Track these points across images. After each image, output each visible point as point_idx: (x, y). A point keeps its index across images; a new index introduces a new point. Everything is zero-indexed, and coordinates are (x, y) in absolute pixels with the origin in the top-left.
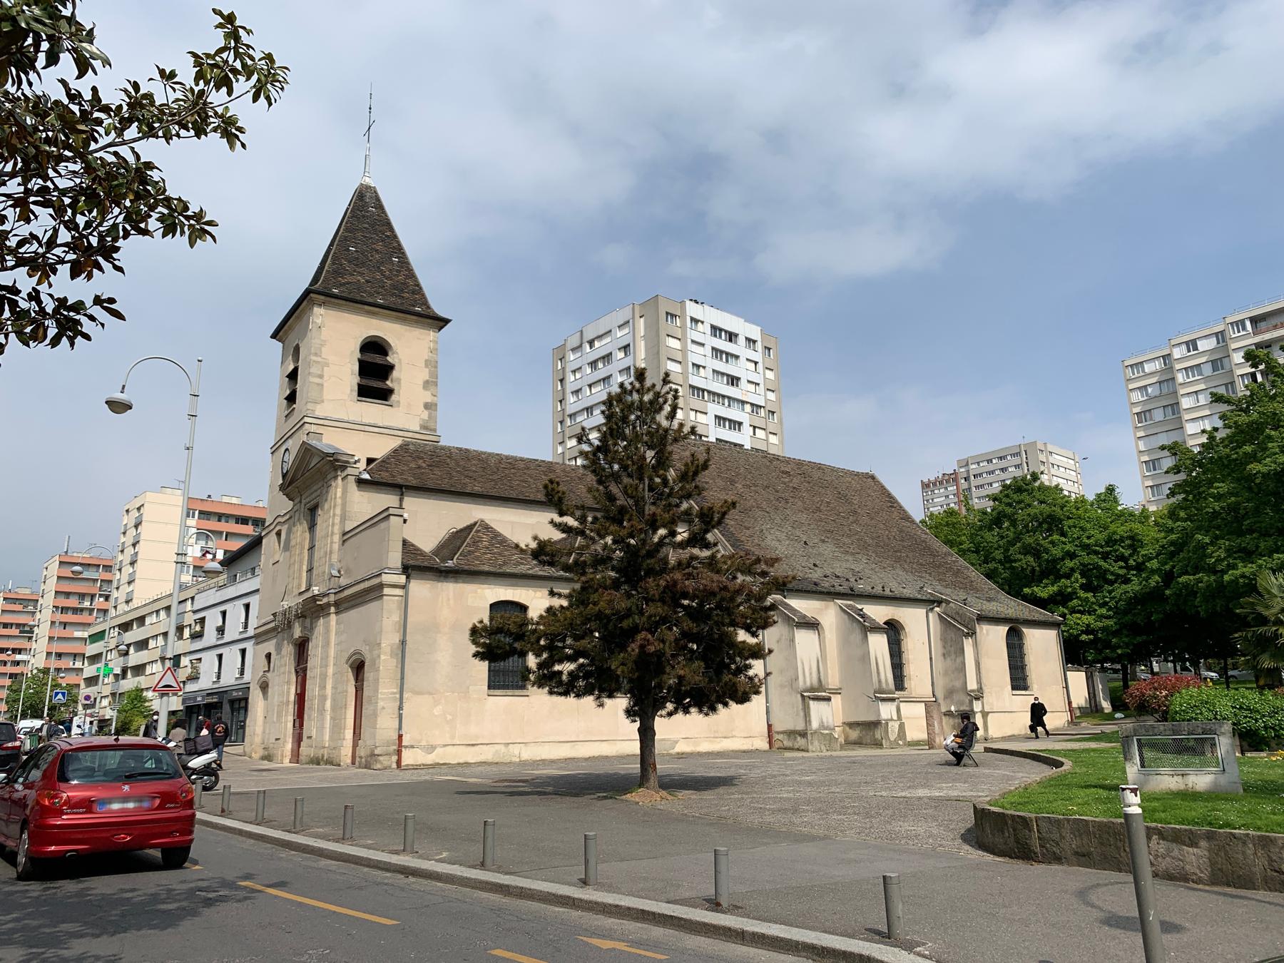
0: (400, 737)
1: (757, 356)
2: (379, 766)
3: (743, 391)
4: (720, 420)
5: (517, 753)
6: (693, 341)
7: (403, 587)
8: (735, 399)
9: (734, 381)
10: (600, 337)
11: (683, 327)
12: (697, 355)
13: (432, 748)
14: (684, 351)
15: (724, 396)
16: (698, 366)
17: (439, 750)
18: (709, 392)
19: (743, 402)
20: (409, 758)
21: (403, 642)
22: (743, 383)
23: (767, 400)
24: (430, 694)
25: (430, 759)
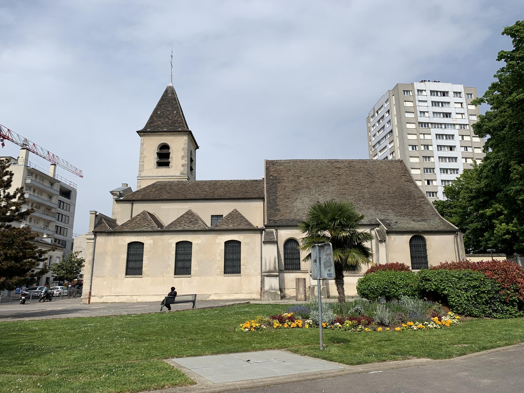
0: (90, 293)
1: (463, 100)
2: (82, 303)
3: (455, 119)
4: (439, 136)
5: (135, 299)
6: (419, 101)
7: (94, 239)
8: (448, 124)
9: (447, 115)
10: (380, 109)
11: (414, 94)
12: (422, 107)
13: (102, 297)
14: (415, 106)
15: (441, 124)
16: (424, 112)
17: (104, 298)
18: (432, 123)
19: (454, 125)
20: (93, 300)
21: (93, 259)
22: (453, 115)
23: (470, 121)
24: (102, 277)
25: (101, 301)
